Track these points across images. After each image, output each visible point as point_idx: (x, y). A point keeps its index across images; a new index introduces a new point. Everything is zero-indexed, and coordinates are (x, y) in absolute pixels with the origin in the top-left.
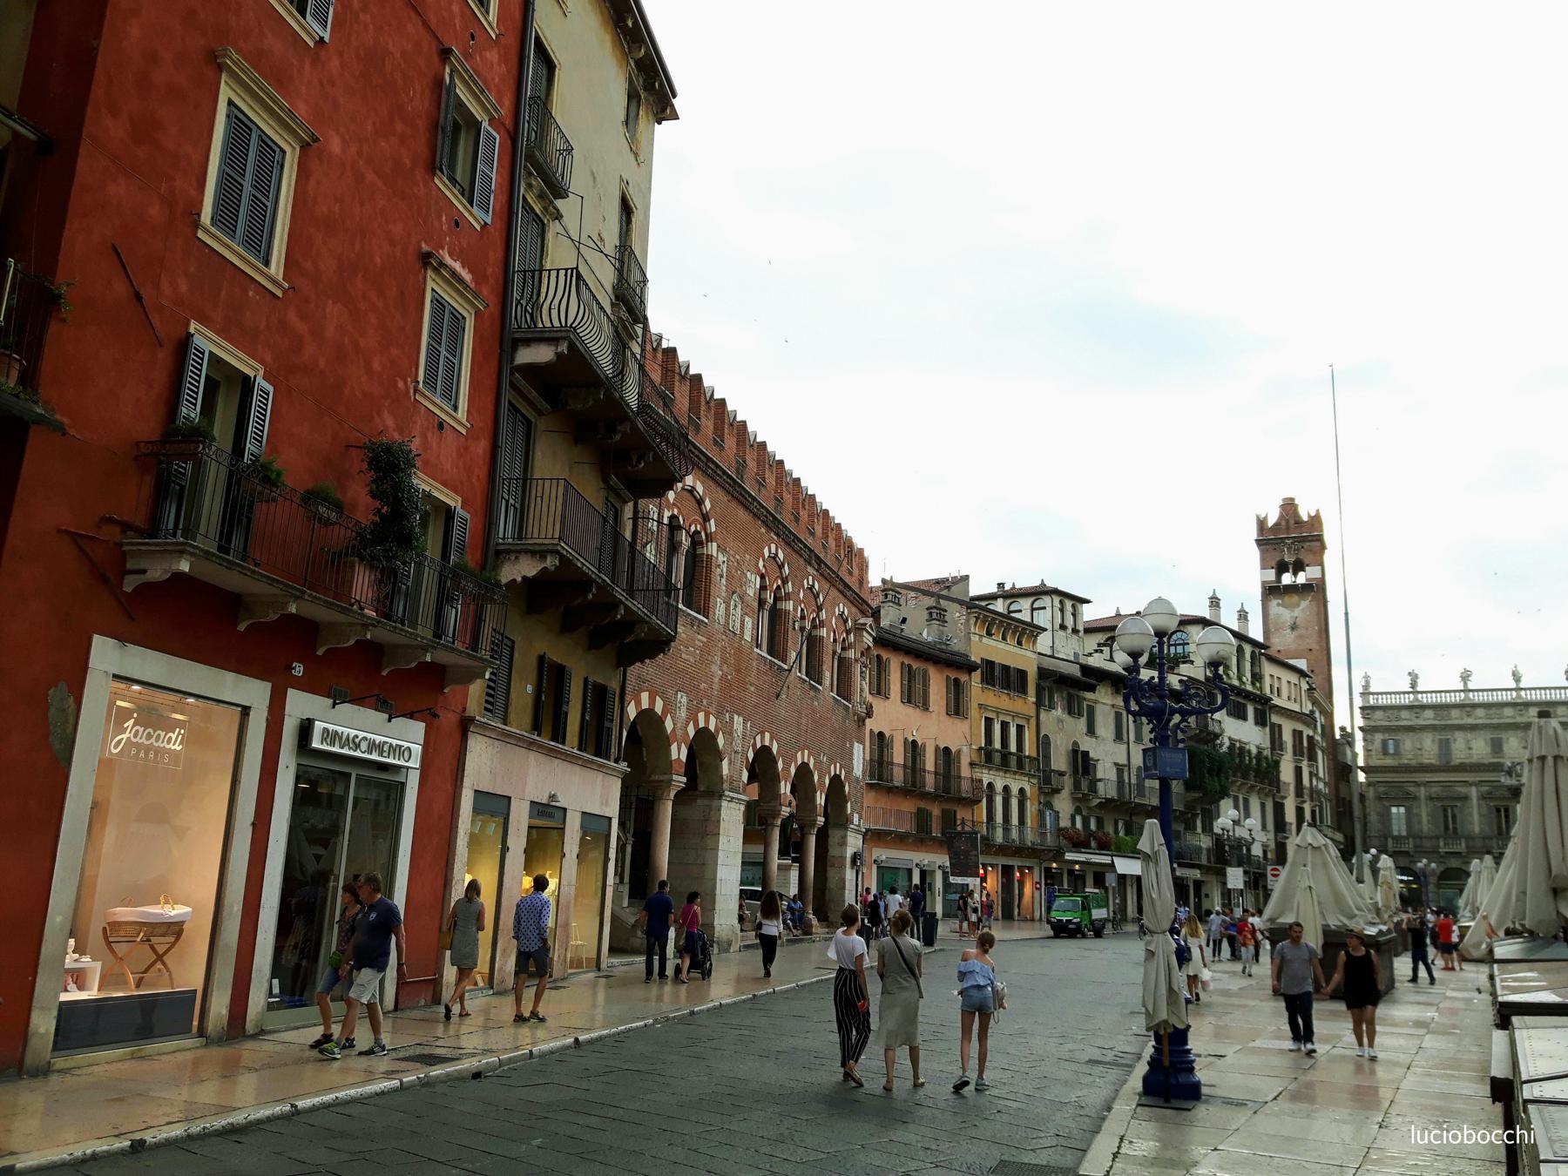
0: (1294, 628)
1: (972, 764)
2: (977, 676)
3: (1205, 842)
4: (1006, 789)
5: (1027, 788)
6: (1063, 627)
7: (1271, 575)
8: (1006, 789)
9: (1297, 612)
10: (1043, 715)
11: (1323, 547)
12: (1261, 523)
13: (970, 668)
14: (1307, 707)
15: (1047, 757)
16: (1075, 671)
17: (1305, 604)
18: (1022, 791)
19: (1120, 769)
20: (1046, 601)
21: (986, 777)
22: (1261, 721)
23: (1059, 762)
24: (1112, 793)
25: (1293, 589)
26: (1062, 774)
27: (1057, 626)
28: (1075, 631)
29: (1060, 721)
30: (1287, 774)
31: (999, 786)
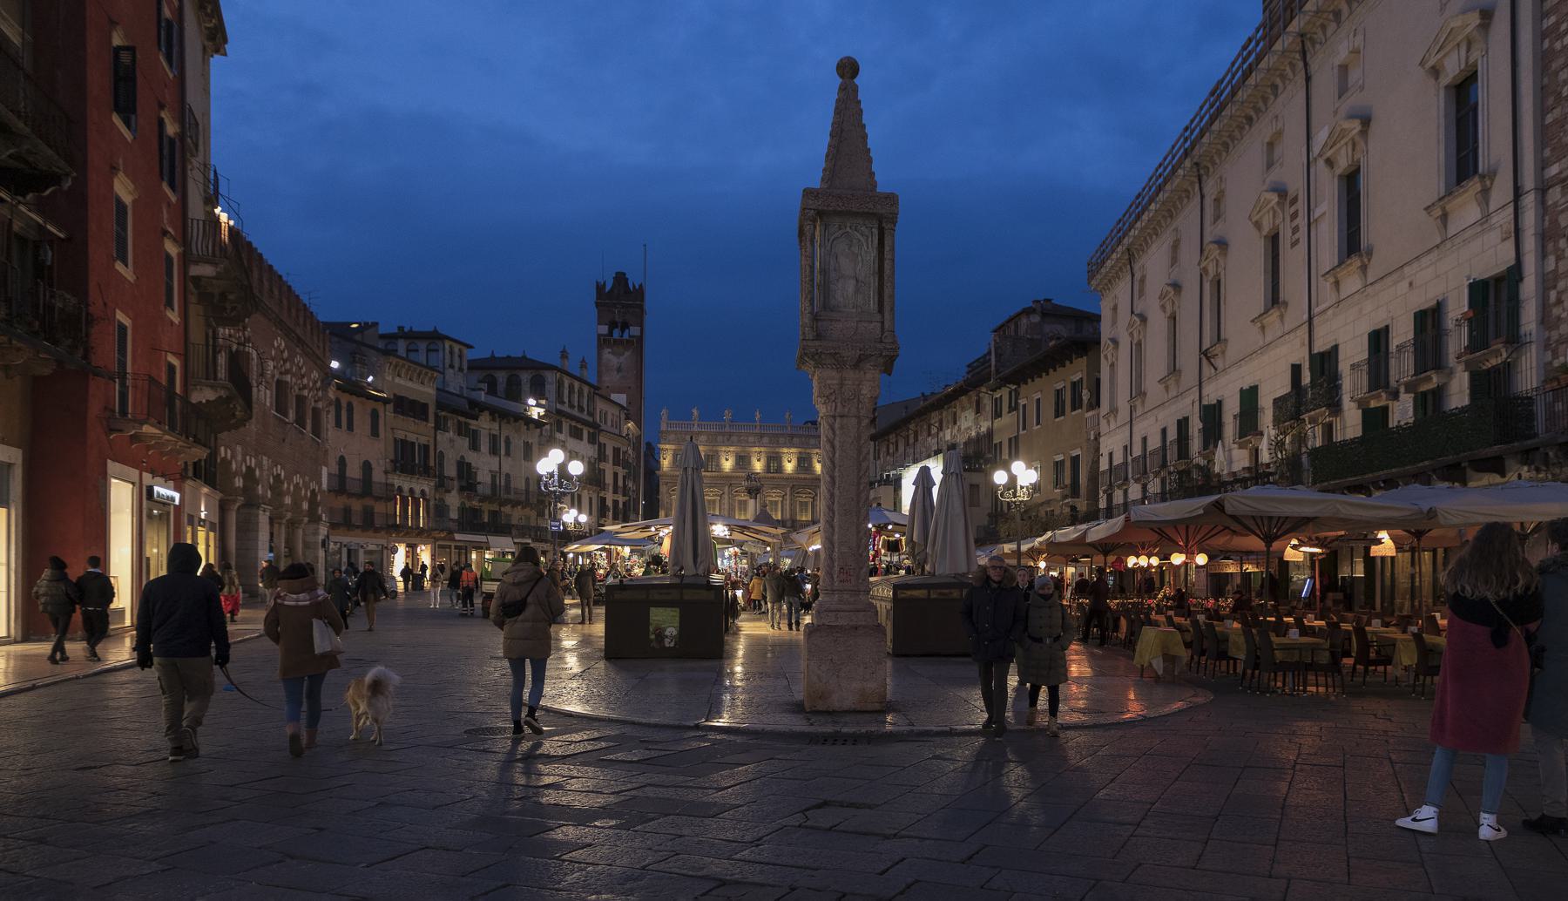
0: (619, 370)
1: (386, 472)
6: (452, 366)
7: (604, 329)
8: (412, 491)
9: (622, 359)
12: (600, 288)
15: (441, 465)
17: (627, 354)
18: (423, 492)
20: (440, 343)
21: (398, 481)
22: (593, 440)
23: (451, 470)
24: (488, 492)
28: (461, 369)
29: (451, 441)
31: (406, 488)
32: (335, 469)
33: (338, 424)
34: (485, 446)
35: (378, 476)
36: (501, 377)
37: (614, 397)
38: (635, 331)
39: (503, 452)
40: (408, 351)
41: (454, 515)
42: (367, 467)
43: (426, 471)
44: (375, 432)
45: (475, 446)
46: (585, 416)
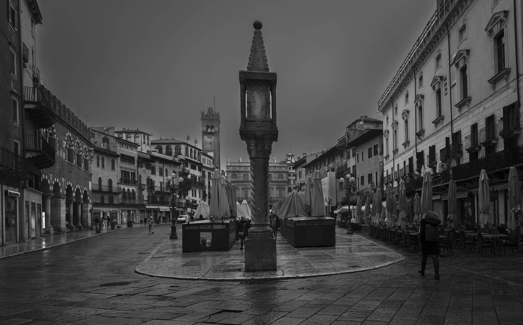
0: (210, 144)
1: (118, 183)
2: (119, 158)
3: (184, 201)
4: (128, 190)
5: (135, 189)
6: (144, 143)
7: (205, 129)
8: (128, 190)
9: (211, 140)
10: (139, 169)
11: (220, 122)
12: (203, 114)
13: (117, 156)
14: (212, 166)
15: (140, 180)
16: (148, 157)
17: (213, 138)
18: (133, 190)
19: (161, 183)
20: (140, 135)
22: (200, 170)
23: (144, 182)
24: (159, 190)
25: (211, 133)
26: (145, 185)
27: (143, 143)
28: (148, 144)
29: (144, 171)
30: (207, 184)
32: (97, 182)
33: (98, 165)
34: (157, 173)
35: (115, 185)
36: (164, 147)
37: (209, 154)
38: (216, 129)
39: (165, 175)
40: (127, 137)
41: (146, 198)
42: (110, 181)
43: (134, 183)
44: (113, 168)
45: (153, 173)
46: (197, 161)
